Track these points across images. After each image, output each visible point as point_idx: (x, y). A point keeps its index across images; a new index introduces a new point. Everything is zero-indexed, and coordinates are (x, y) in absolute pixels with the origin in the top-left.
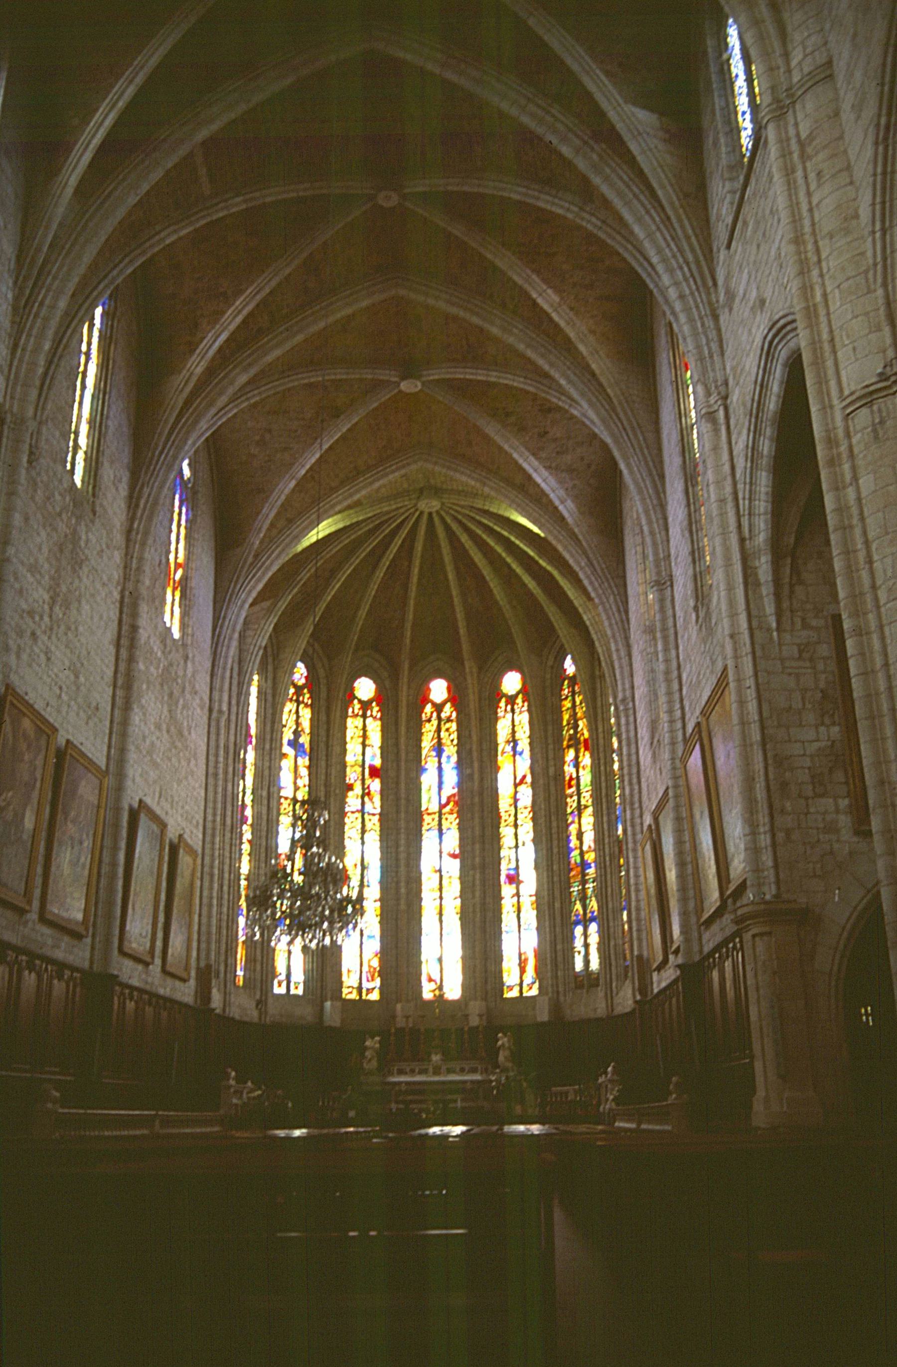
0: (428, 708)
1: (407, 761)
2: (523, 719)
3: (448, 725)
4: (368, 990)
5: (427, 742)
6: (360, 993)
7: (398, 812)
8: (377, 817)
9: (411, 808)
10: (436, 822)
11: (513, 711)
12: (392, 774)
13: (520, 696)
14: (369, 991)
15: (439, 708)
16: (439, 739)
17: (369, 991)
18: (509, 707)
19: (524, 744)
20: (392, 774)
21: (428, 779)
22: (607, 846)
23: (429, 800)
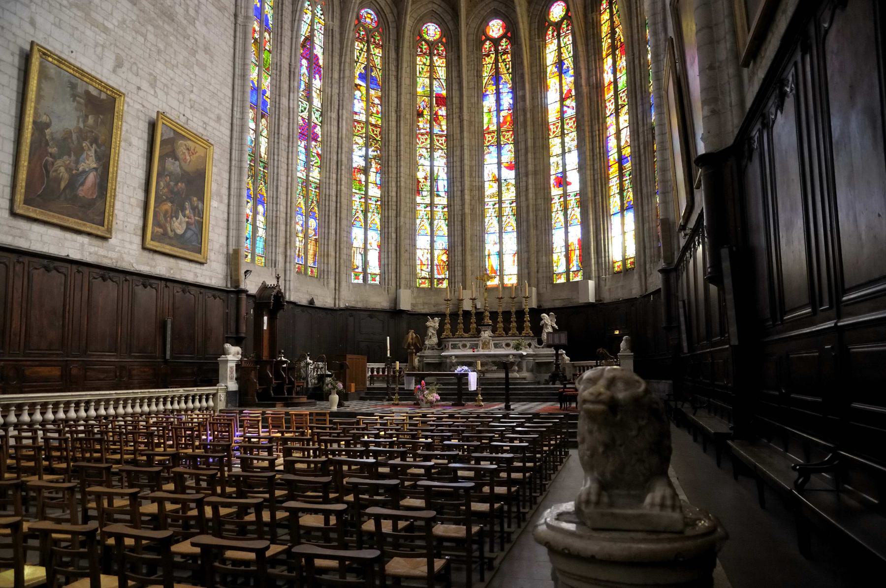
0: (487, 45)
1: (468, 88)
2: (568, 40)
3: (504, 57)
4: (439, 279)
5: (487, 72)
6: (431, 283)
7: (462, 131)
8: (444, 138)
9: (473, 128)
10: (495, 139)
11: (559, 36)
12: (456, 100)
13: (565, 22)
14: (440, 281)
15: (496, 42)
16: (497, 68)
17: (440, 281)
18: (555, 33)
19: (569, 63)
20: (456, 100)
21: (489, 102)
22: (641, 135)
23: (489, 121)
